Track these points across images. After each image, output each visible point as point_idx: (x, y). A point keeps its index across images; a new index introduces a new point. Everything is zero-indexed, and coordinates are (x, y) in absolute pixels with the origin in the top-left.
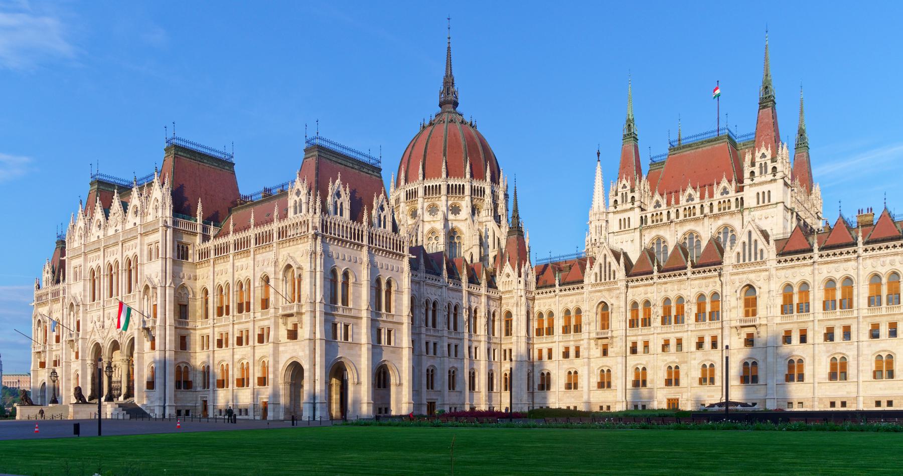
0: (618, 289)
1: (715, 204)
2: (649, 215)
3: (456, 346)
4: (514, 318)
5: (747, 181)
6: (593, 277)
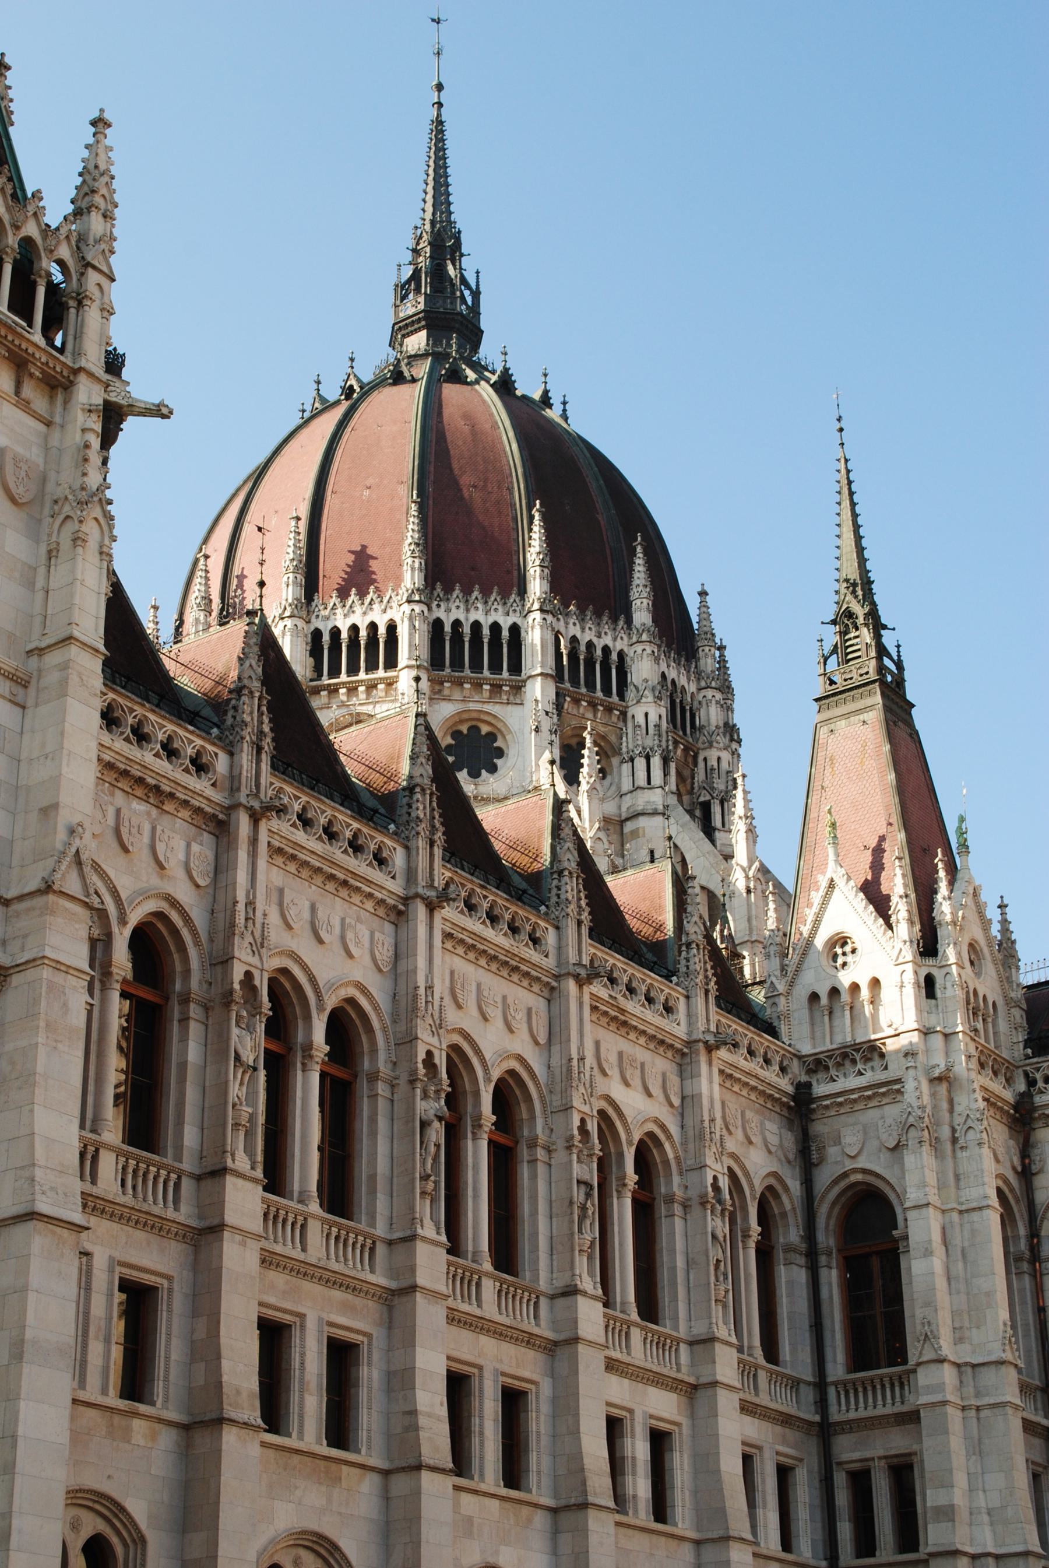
3: (513, 1401)
4: (923, 1227)
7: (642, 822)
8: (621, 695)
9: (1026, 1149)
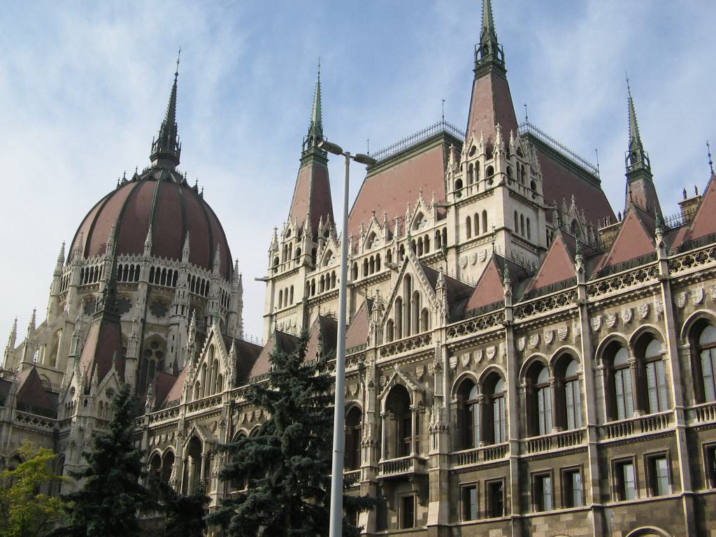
2: (318, 279)
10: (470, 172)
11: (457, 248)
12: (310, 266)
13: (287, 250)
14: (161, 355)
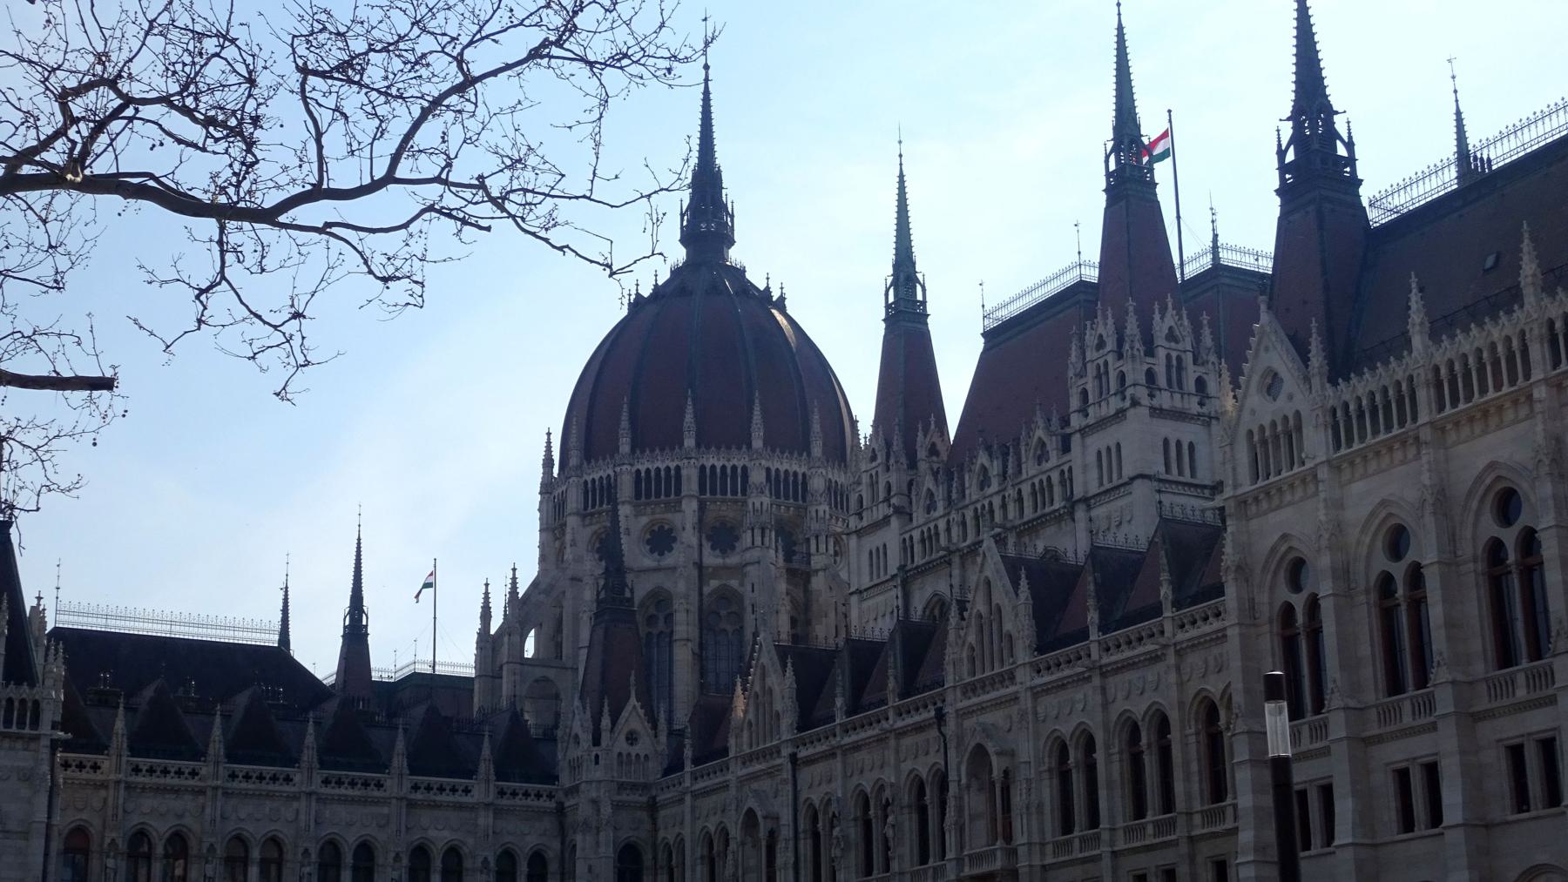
0: (779, 768)
1: (1026, 489)
2: (916, 534)
5: (1076, 421)
6: (746, 734)
7: (749, 568)
8: (744, 492)
9: (654, 820)
10: (1099, 376)
11: (1086, 500)
12: (904, 513)
13: (873, 484)
14: (739, 616)
